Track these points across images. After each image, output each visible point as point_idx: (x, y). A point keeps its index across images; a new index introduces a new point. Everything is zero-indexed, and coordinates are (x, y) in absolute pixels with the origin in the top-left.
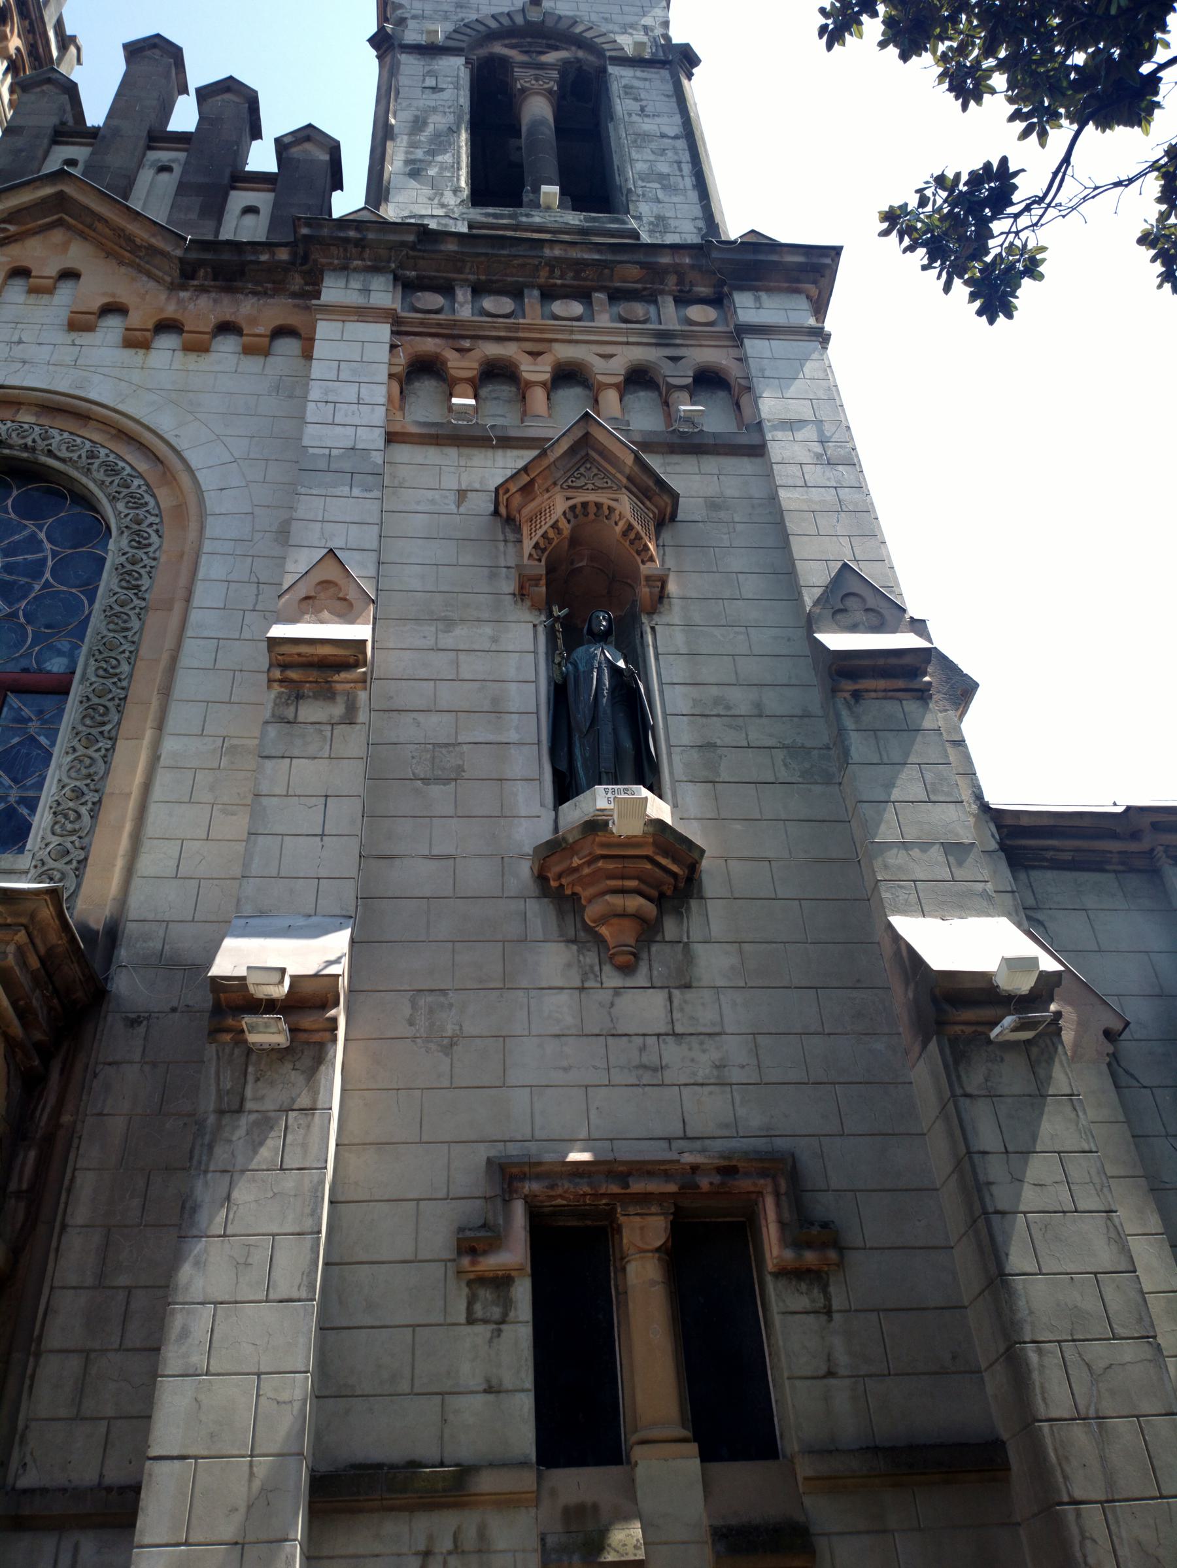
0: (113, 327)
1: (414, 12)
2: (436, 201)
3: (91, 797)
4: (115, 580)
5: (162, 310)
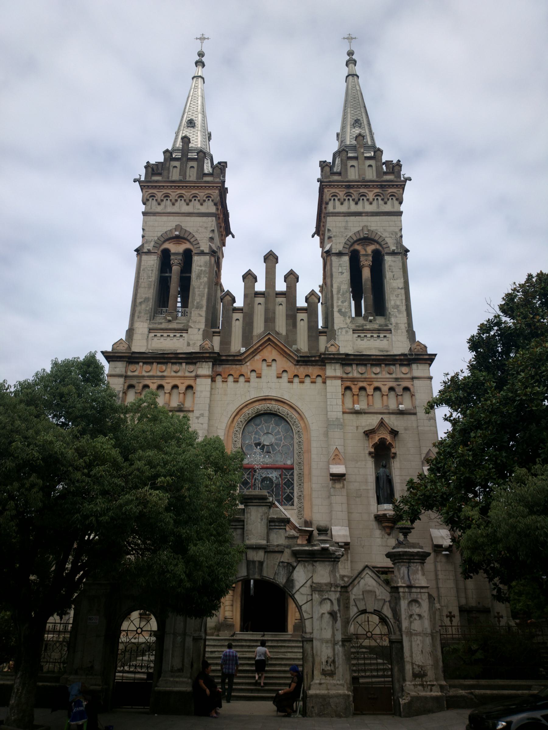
0: (285, 376)
1: (334, 234)
3: (302, 496)
4: (297, 446)
5: (294, 372)
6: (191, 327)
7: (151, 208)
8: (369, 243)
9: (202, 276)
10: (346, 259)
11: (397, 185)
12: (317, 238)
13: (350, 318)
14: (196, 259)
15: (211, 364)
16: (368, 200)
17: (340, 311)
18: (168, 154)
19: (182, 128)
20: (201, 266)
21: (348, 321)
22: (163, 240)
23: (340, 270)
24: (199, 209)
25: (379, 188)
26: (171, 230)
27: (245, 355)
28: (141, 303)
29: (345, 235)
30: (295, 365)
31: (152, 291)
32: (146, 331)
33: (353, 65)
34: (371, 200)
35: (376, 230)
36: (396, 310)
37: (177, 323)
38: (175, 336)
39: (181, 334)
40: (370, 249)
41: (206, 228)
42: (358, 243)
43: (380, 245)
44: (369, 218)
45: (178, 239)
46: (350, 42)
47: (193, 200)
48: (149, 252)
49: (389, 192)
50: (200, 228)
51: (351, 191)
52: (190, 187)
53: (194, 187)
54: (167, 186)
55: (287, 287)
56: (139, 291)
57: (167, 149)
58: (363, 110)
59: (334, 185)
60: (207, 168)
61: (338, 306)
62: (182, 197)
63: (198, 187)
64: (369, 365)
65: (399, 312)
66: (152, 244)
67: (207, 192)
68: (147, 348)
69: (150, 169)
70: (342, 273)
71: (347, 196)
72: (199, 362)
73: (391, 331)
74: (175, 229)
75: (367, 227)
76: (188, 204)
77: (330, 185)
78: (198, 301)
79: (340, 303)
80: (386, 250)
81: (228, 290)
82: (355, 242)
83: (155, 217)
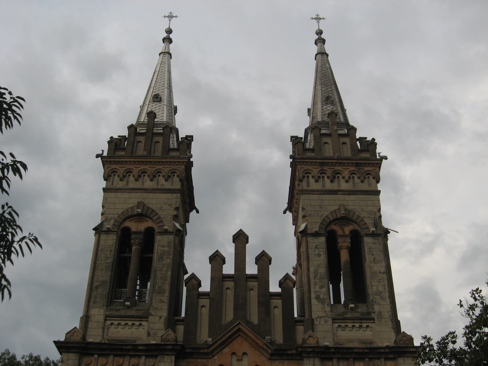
1: (309, 212)
2: (323, 310)
6: (152, 315)
7: (112, 184)
8: (347, 223)
9: (165, 257)
10: (323, 239)
11: (373, 164)
12: (289, 215)
13: (330, 306)
14: (158, 238)
15: (173, 358)
16: (343, 178)
17: (318, 298)
18: (133, 129)
19: (147, 103)
20: (163, 246)
21: (328, 309)
22: (123, 217)
23: (317, 252)
24: (163, 185)
25: (355, 166)
26: (132, 208)
27: (213, 348)
28: (97, 287)
30: (269, 359)
31: (109, 273)
32: (102, 318)
33: (322, 44)
34: (347, 178)
36: (378, 297)
37: (136, 310)
38: (133, 324)
39: (141, 322)
40: (347, 230)
41: (170, 205)
42: (335, 222)
43: (359, 226)
44: (346, 196)
45: (140, 217)
46: (318, 22)
47: (157, 175)
48: (108, 231)
50: (162, 205)
51: (326, 168)
52: (155, 162)
53: (159, 162)
54: (131, 162)
55: (259, 269)
56: (96, 273)
57: (132, 124)
58: (334, 88)
59: (307, 162)
60: (173, 144)
61: (315, 292)
62: (146, 172)
63: (163, 162)
64: (352, 360)
65: (382, 298)
66: (112, 222)
67: (172, 167)
68: (103, 338)
69: (113, 145)
70: (319, 255)
71: (321, 174)
72: (161, 355)
73: (374, 320)
74: (137, 206)
75: (344, 206)
76: (151, 180)
77: (303, 162)
78: (160, 285)
79: (317, 288)
80: (366, 231)
81: (193, 273)
82: (331, 222)
83: (116, 194)
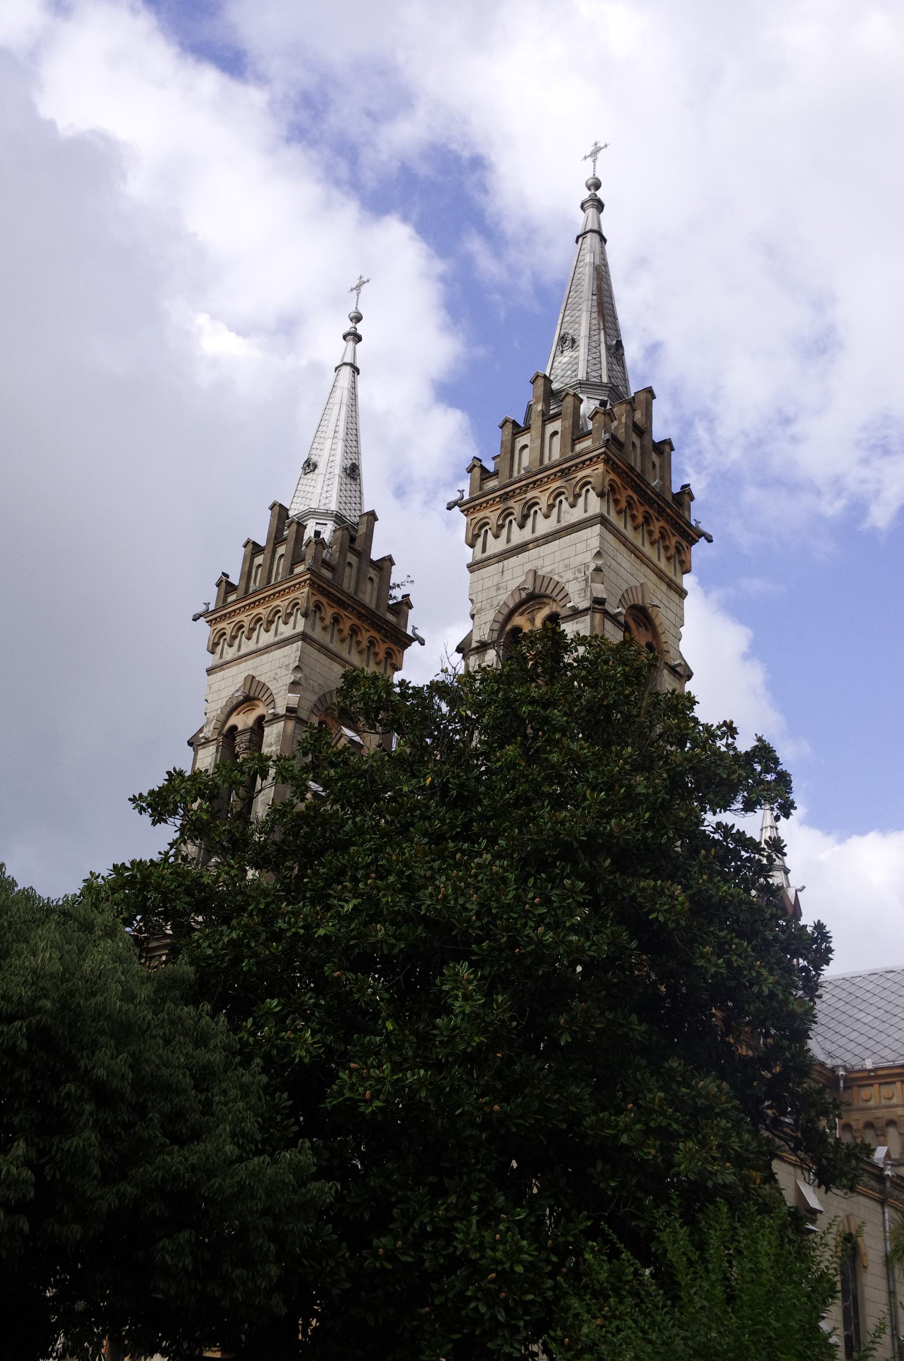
8: (541, 603)
11: (590, 459)
29: (495, 603)
35: (551, 572)
49: (578, 479)
51: (511, 503)
52: (269, 596)
53: (274, 594)
54: (239, 609)
59: (480, 505)
77: (474, 507)
82: (512, 613)
